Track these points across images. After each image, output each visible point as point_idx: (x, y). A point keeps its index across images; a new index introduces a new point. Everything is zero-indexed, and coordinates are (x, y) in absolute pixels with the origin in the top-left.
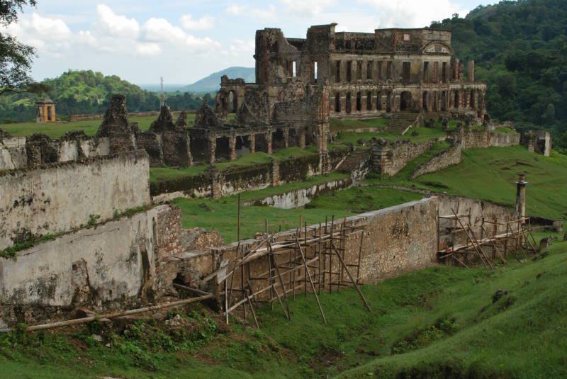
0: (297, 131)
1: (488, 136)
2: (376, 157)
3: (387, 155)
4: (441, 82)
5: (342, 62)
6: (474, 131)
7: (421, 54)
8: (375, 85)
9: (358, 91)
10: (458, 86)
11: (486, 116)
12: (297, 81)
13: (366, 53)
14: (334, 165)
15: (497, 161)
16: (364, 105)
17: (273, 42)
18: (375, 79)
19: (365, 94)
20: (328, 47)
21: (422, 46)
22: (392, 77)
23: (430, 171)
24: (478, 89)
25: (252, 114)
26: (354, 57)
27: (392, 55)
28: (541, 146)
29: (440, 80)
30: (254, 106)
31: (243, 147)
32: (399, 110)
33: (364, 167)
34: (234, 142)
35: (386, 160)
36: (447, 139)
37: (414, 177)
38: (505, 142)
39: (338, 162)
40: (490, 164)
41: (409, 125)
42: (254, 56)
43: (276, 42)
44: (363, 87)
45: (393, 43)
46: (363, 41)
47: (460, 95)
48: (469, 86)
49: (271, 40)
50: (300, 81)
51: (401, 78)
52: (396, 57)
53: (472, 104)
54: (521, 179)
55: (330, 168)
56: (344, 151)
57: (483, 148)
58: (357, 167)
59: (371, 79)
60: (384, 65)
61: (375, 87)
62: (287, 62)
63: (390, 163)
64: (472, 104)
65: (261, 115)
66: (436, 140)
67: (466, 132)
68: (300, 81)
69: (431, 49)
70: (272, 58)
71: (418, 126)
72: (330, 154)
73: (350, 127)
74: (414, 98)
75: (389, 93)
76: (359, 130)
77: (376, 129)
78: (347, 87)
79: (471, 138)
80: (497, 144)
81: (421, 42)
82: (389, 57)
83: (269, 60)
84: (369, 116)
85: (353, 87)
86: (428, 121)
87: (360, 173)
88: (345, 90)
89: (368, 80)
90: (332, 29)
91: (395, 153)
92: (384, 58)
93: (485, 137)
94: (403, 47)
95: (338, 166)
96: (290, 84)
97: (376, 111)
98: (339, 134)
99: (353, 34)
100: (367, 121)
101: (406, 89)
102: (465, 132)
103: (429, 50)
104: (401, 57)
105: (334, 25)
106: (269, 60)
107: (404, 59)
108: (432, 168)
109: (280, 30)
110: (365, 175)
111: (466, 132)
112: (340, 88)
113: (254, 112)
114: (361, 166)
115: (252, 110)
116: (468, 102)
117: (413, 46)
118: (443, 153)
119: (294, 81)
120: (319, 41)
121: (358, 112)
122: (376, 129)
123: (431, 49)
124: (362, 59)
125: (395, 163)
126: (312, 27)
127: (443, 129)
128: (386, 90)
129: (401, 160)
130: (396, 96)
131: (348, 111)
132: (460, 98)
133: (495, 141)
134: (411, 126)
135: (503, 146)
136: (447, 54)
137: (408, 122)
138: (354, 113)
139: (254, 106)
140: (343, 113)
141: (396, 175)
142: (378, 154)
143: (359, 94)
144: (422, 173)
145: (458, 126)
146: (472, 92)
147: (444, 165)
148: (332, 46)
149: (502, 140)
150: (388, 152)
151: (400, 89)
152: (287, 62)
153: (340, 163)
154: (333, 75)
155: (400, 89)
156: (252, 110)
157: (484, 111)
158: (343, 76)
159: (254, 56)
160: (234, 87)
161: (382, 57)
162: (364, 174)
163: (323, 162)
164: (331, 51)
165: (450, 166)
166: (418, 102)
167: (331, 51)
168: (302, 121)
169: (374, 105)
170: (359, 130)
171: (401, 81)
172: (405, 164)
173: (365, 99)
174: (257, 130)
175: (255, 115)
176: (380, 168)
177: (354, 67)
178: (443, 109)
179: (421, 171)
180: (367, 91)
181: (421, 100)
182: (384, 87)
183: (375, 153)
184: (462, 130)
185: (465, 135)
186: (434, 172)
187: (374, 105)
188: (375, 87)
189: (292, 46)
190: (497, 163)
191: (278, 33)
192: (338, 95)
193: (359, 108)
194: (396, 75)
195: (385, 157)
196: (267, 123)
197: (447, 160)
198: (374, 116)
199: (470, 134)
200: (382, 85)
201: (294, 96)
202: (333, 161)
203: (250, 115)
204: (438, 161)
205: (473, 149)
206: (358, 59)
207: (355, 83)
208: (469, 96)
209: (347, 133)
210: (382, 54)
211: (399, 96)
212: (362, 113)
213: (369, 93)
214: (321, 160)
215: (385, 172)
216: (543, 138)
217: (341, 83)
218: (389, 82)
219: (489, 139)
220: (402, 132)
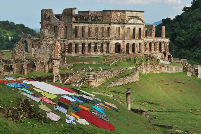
0: (45, 63)
2: (87, 77)
3: (93, 76)
4: (138, 38)
5: (79, 27)
6: (151, 64)
7: (125, 24)
8: (99, 39)
9: (89, 42)
10: (151, 40)
11: (169, 56)
12: (50, 37)
13: (93, 23)
14: (63, 81)
15: (162, 80)
16: (93, 50)
17: (48, 16)
18: (100, 36)
19: (93, 44)
20: (71, 19)
21: (125, 19)
22: (110, 35)
23: (118, 85)
24: (164, 42)
25: (18, 54)
26: (87, 26)
27: (110, 24)
28: (196, 73)
29: (137, 37)
30: (19, 50)
31: (10, 71)
32: (114, 52)
33: (80, 82)
34: (3, 69)
35: (92, 79)
36: (133, 68)
37: (107, 88)
38: (172, 70)
39: (66, 79)
40: (158, 82)
41: (115, 60)
42: (40, 23)
43: (50, 16)
45: (111, 17)
46: (96, 16)
47: (153, 45)
48: (158, 40)
49: (47, 15)
50: (52, 37)
51: (115, 36)
52: (112, 25)
53: (160, 49)
54: (128, 91)
55: (61, 82)
56: (70, 74)
57: (157, 74)
58: (75, 82)
59: (97, 36)
60: (105, 29)
62: (54, 26)
63: (95, 80)
64: (160, 49)
65: (22, 55)
66: (126, 68)
67: (146, 65)
68: (52, 37)
69: (132, 21)
70: (47, 24)
71: (121, 61)
72: (60, 75)
73: (82, 61)
74: (122, 46)
75: (108, 44)
76: (86, 63)
77: (97, 62)
78: (83, 40)
79: (149, 68)
80: (166, 71)
81: (125, 18)
82: (108, 25)
83: (46, 25)
84: (96, 55)
85: (86, 40)
86: (128, 58)
87: (77, 85)
88: (81, 42)
89: (95, 37)
90: (73, 11)
91: (98, 75)
93: (158, 67)
94: (117, 20)
95: (66, 81)
96: (45, 39)
97: (100, 53)
98: (74, 64)
99: (94, 12)
100: (94, 58)
101: (118, 42)
102: (145, 64)
103: (130, 22)
104: (115, 25)
105: (75, 9)
106: (46, 25)
107: (117, 26)
108: (119, 83)
109: (52, 10)
110: (81, 86)
111: (146, 65)
112: (78, 41)
113: (19, 54)
114: (78, 81)
115: (18, 52)
116: (158, 48)
117: (121, 19)
118: (126, 76)
119: (47, 37)
120: (68, 17)
121: (89, 53)
122: (97, 62)
123: (132, 21)
124: (91, 26)
125: (98, 80)
126: (65, 9)
127: (135, 63)
128: (106, 42)
129: (102, 79)
130: (112, 45)
131: (83, 52)
132: (153, 47)
133: (165, 70)
134: (116, 61)
135: (171, 72)
136: (141, 24)
137: (115, 59)
138: (86, 53)
139: (19, 50)
140: (80, 53)
141: (99, 87)
142: (88, 75)
144: (113, 86)
145: (141, 62)
146: (160, 43)
147: (127, 82)
148: (74, 19)
149: (170, 69)
151: (114, 42)
152: (54, 26)
153: (68, 80)
154: (74, 34)
155: (115, 41)
156: (18, 52)
157: (168, 53)
158: (80, 34)
159: (40, 23)
160: (26, 39)
161: (104, 25)
162: (80, 86)
163: (56, 79)
164: (73, 22)
166: (124, 49)
167: (73, 22)
168: (47, 58)
169: (99, 50)
170: (86, 63)
171: (115, 37)
172: (105, 81)
173: (93, 47)
174: (17, 63)
175: (19, 55)
176: (89, 82)
177: (87, 30)
178: (139, 52)
179: (112, 85)
180: (95, 42)
181: (125, 48)
182: (105, 40)
183: (87, 75)
184: (143, 64)
185: (145, 67)
186: (121, 86)
187: (99, 50)
188: (100, 41)
189: (57, 19)
190: (162, 81)
191: (50, 11)
192: (77, 44)
193: (89, 50)
194: (112, 34)
195: (92, 77)
196: (24, 59)
197: (128, 80)
198: (99, 55)
199: (149, 66)
200: (104, 39)
201: (48, 45)
202: (63, 79)
203: (17, 55)
204: (124, 80)
205: (150, 74)
206: (89, 26)
207: (87, 39)
208: (158, 45)
209: (79, 64)
210: (104, 24)
211: (114, 45)
212: (92, 54)
213: (96, 44)
214: (55, 78)
215: (92, 85)
216: (197, 69)
217: (79, 38)
218: (108, 38)
219: (161, 68)
220: (110, 64)
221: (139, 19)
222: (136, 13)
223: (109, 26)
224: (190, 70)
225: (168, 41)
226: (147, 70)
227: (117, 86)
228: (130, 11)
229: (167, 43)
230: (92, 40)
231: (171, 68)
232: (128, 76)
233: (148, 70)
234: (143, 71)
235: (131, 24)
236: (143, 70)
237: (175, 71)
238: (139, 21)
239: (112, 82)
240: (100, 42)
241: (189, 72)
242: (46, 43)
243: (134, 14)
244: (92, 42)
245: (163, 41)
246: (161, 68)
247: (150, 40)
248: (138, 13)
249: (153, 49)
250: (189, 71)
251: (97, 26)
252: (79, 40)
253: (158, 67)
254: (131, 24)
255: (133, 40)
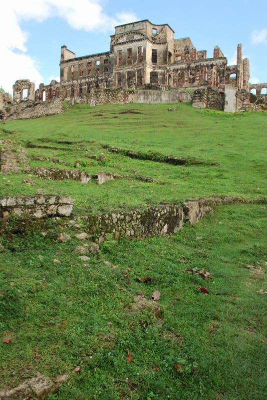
1: (125, 94)
8: (92, 77)
9: (79, 83)
23: (23, 117)
44: (83, 81)
61: (93, 79)
69: (124, 39)
85: (75, 82)
92: (100, 58)
102: (95, 92)
103: (120, 41)
123: (124, 39)
124: (82, 63)
143: (81, 85)
147: (39, 115)
150: (7, 108)
165: (47, 115)
180: (86, 82)
182: (100, 78)
188: (93, 79)
213: (88, 84)
218: (105, 74)
219: (126, 96)
221: (137, 34)
222: (132, 25)
223: (107, 58)
224: (200, 96)
225: (223, 63)
226: (98, 100)
227: (21, 119)
228: (122, 26)
229: (221, 66)
230: (83, 80)
231: (155, 96)
232: (39, 105)
233: (100, 100)
234: (92, 102)
235: (120, 44)
236: (92, 100)
237: (167, 101)
238: (137, 37)
239: (15, 113)
240: (94, 82)
241: (197, 100)
242: (18, 88)
243: (129, 28)
244: (83, 83)
245: (210, 64)
246: (127, 96)
247: (179, 66)
248: (135, 25)
249: (187, 81)
250: (198, 98)
251: (90, 61)
252: (67, 83)
253: (121, 95)
254: (120, 44)
255: (127, 68)
